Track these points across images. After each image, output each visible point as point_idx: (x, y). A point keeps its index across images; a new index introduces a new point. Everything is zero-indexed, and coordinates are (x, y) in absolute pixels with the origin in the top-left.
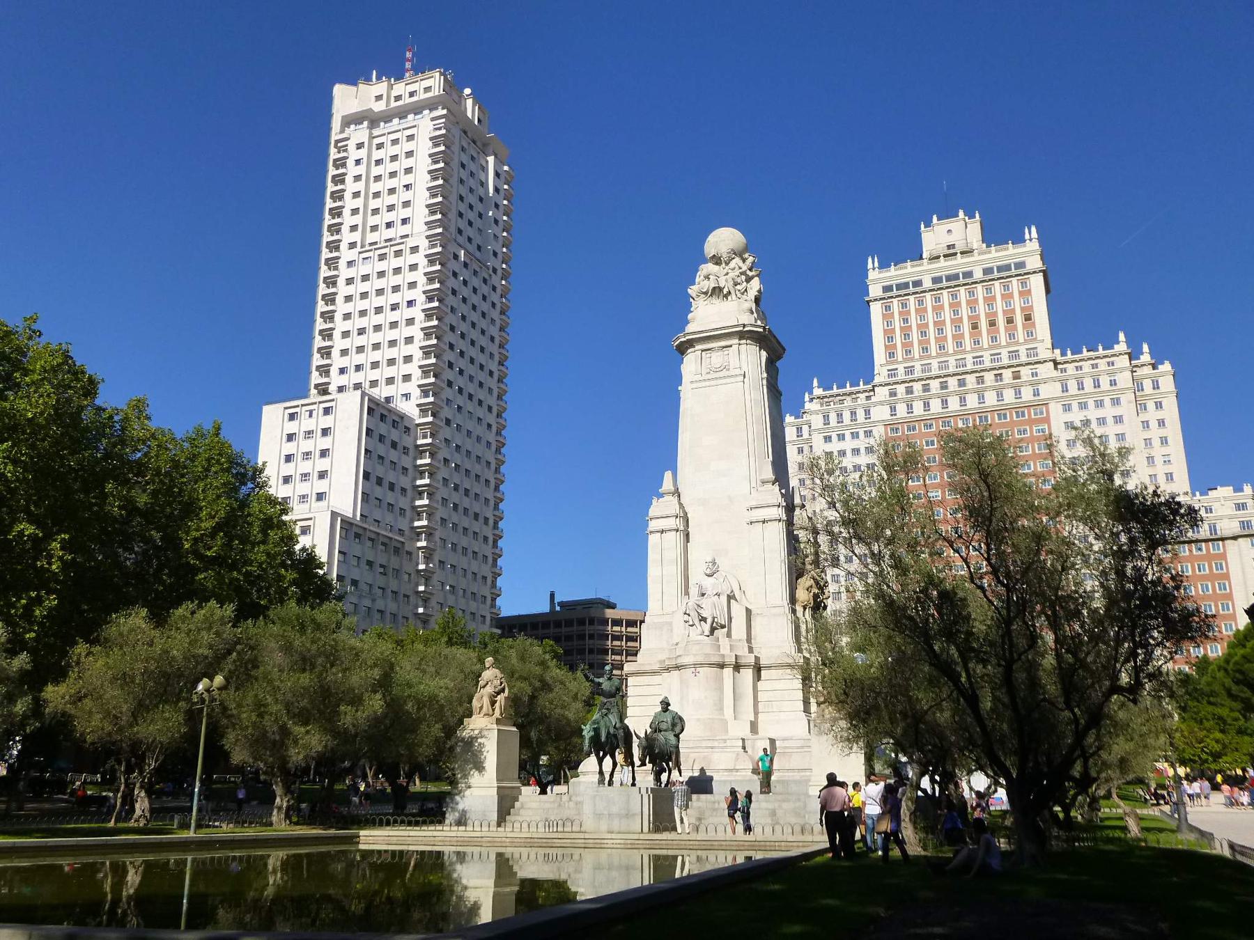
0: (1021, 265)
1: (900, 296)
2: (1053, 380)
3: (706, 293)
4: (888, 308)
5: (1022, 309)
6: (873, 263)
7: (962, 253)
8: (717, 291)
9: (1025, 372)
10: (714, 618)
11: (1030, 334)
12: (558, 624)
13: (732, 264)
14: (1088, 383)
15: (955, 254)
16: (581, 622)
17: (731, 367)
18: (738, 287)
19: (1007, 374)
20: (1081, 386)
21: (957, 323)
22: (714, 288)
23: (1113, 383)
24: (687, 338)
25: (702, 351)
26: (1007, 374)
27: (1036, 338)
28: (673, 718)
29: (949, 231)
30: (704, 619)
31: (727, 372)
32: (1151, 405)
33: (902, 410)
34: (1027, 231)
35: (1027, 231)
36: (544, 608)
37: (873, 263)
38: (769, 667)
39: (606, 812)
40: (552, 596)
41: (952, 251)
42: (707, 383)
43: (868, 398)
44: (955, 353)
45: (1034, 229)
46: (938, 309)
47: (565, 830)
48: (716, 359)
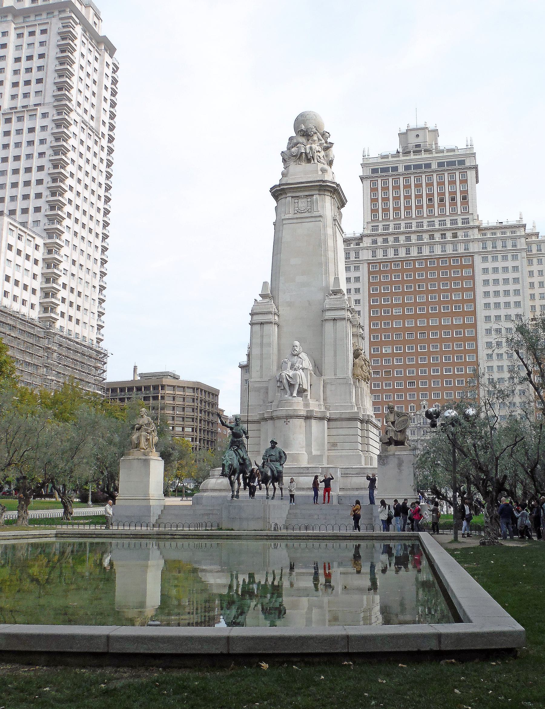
0: (462, 162)
2: (478, 240)
4: (375, 184)
7: (425, 151)
8: (304, 155)
9: (460, 234)
10: (299, 385)
12: (139, 389)
13: (315, 138)
14: (499, 244)
15: (421, 151)
16: (156, 387)
18: (318, 154)
19: (449, 235)
20: (494, 247)
21: (419, 197)
22: (302, 153)
23: (514, 245)
24: (281, 187)
26: (449, 235)
28: (280, 453)
29: (418, 136)
30: (291, 386)
31: (309, 214)
32: (535, 261)
33: (380, 254)
36: (131, 378)
38: (335, 420)
39: (237, 517)
40: (135, 368)
41: (418, 149)
42: (295, 221)
43: (358, 244)
44: (439, 216)
46: (407, 187)
47: (213, 528)
48: (302, 204)
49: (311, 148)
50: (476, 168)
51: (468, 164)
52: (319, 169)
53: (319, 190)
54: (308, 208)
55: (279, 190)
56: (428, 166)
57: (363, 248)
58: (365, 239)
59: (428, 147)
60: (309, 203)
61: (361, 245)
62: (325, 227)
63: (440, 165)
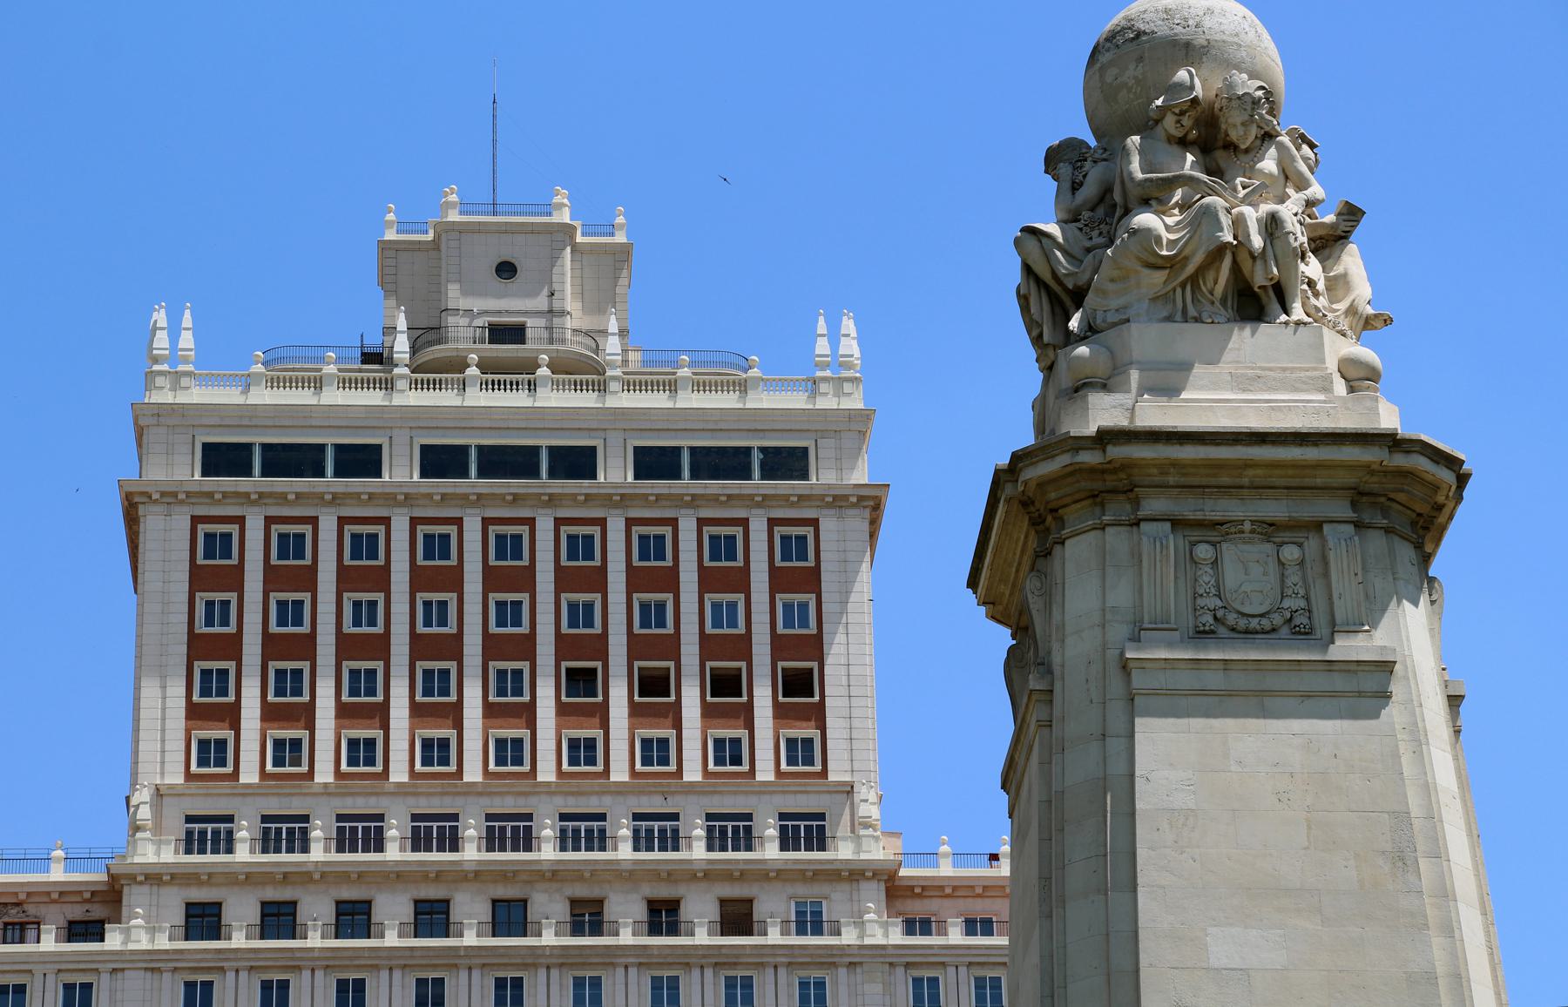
1: (282, 498)
3: (1171, 264)
4: (218, 545)
5: (779, 646)
6: (174, 332)
11: (800, 751)
13: (1269, 164)
15: (530, 366)
17: (1322, 629)
22: (1223, 248)
24: (1116, 452)
25: (1177, 524)
27: (824, 773)
29: (506, 270)
34: (822, 327)
35: (822, 327)
37: (174, 332)
43: (86, 929)
45: (849, 325)
49: (1272, 225)
50: (871, 503)
51: (823, 477)
52: (1332, 365)
53: (1359, 496)
54: (1286, 603)
55: (1092, 471)
56: (577, 462)
57: (120, 965)
58: (137, 903)
59: (576, 346)
60: (1294, 577)
61: (114, 940)
62: (1419, 740)
63: (655, 463)
